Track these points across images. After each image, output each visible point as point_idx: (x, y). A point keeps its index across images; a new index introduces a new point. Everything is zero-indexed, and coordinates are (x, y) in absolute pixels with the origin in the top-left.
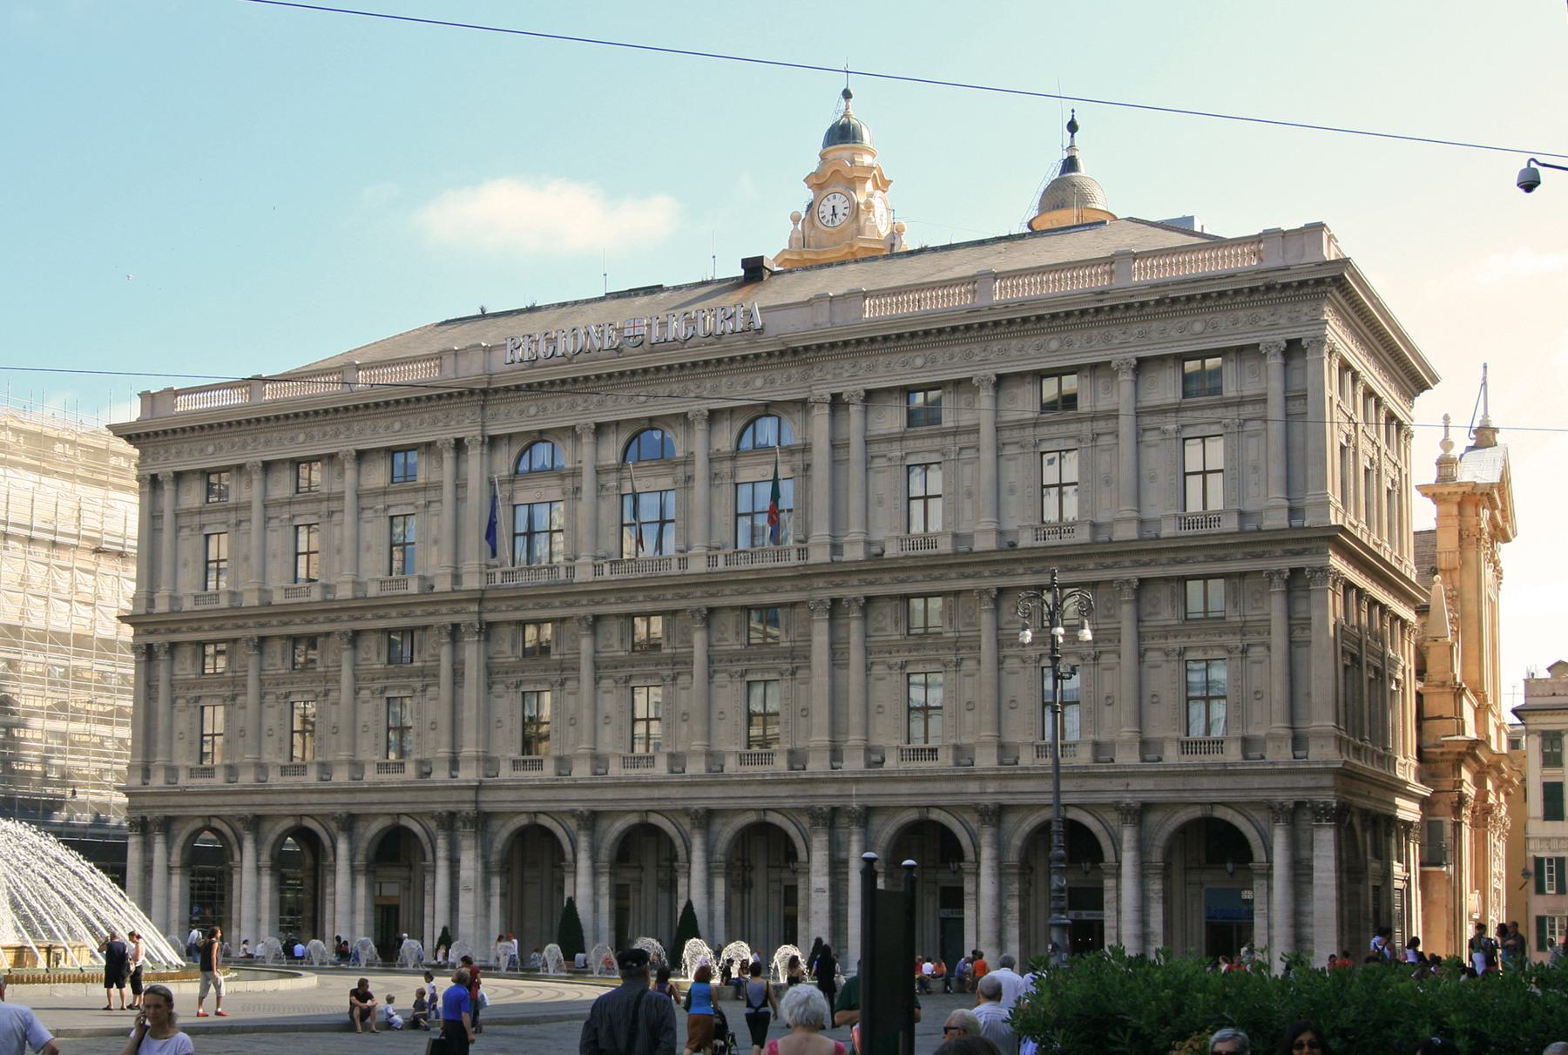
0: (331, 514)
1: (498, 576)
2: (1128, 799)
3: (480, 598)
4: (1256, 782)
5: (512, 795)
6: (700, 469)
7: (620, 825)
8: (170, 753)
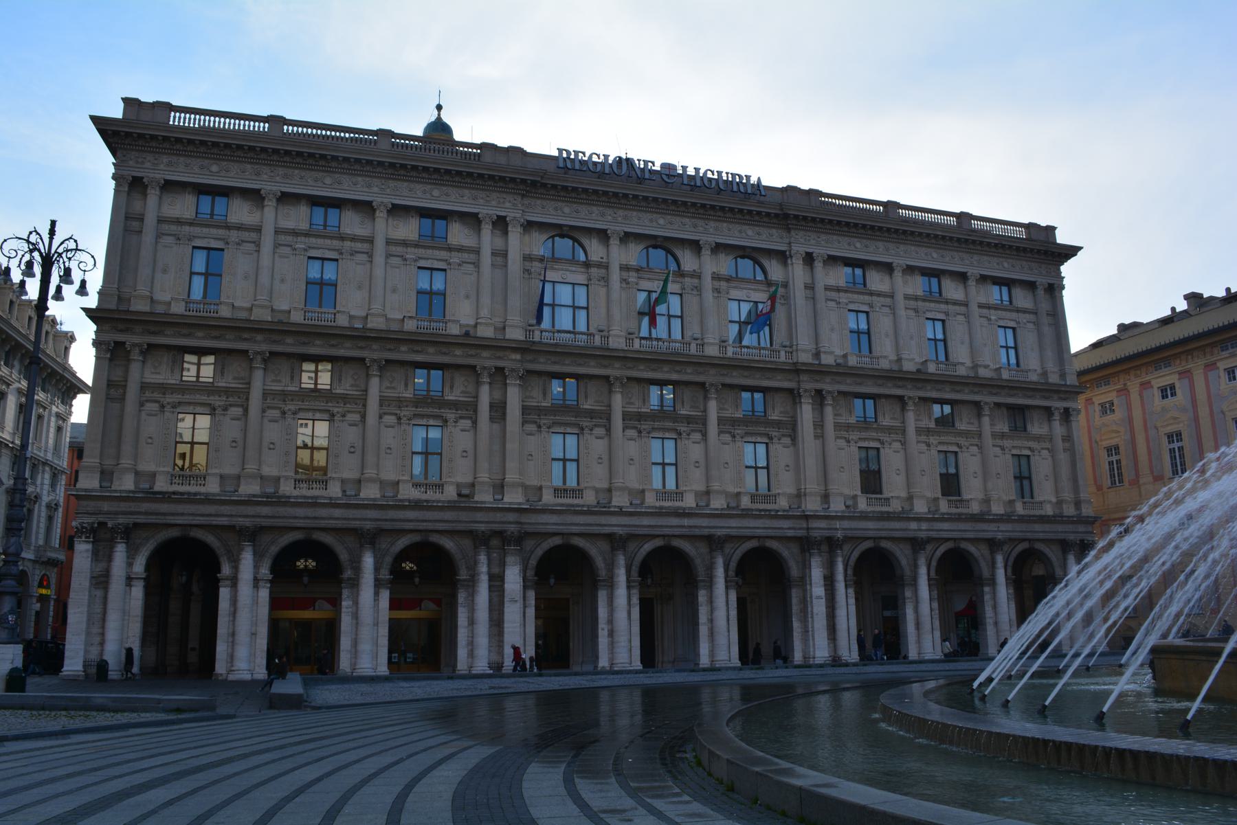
0: (353, 253)
1: (537, 333)
2: (1000, 536)
3: (526, 349)
4: (1060, 528)
5: (554, 519)
6: (708, 283)
7: (648, 547)
8: (136, 457)
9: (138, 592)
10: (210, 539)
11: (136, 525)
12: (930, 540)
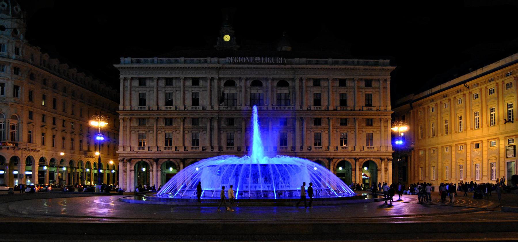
2: (358, 157)
9: (133, 173)
10: (147, 161)
11: (131, 159)
12: (334, 158)
